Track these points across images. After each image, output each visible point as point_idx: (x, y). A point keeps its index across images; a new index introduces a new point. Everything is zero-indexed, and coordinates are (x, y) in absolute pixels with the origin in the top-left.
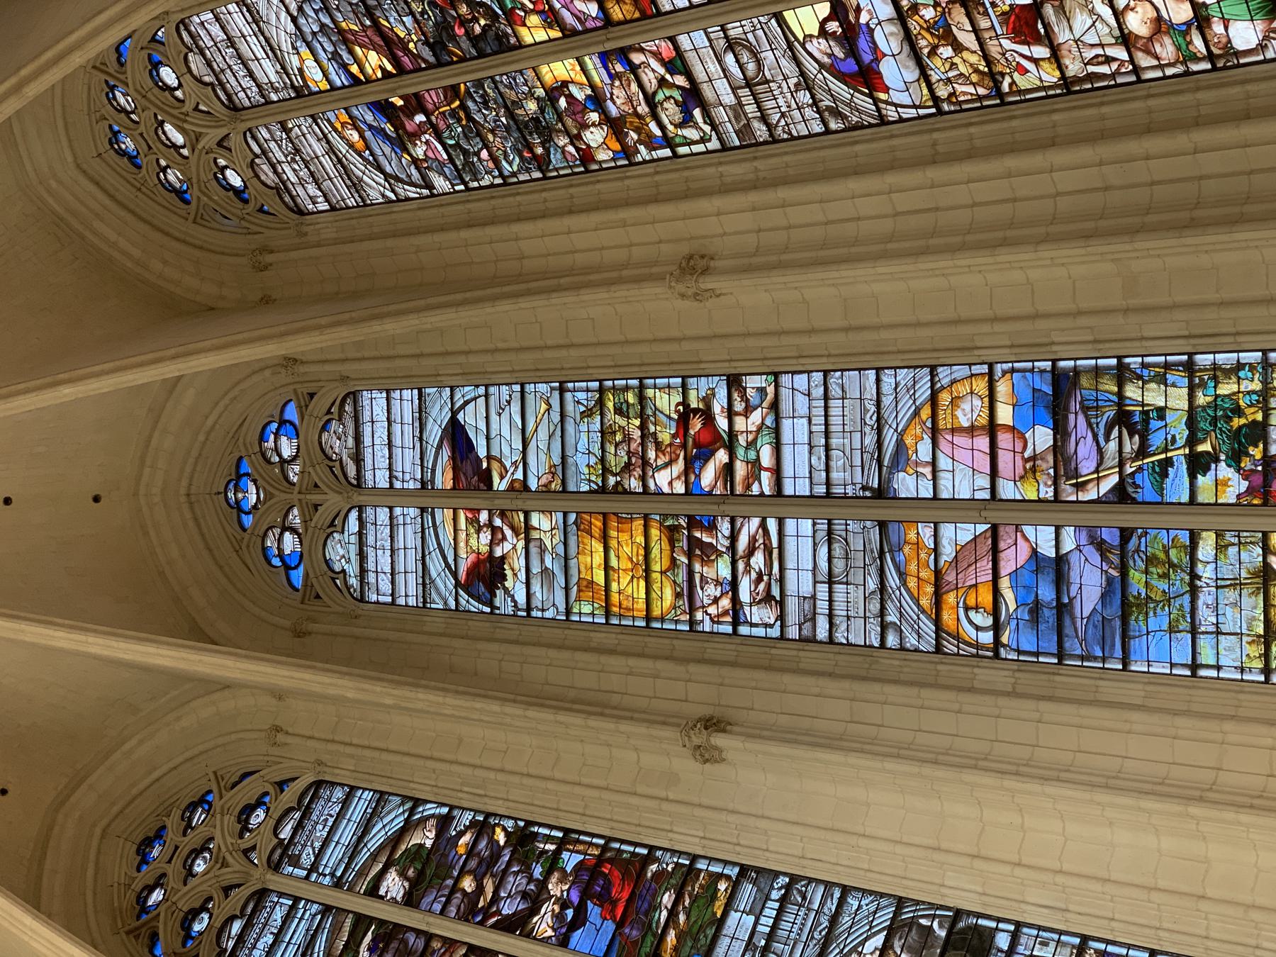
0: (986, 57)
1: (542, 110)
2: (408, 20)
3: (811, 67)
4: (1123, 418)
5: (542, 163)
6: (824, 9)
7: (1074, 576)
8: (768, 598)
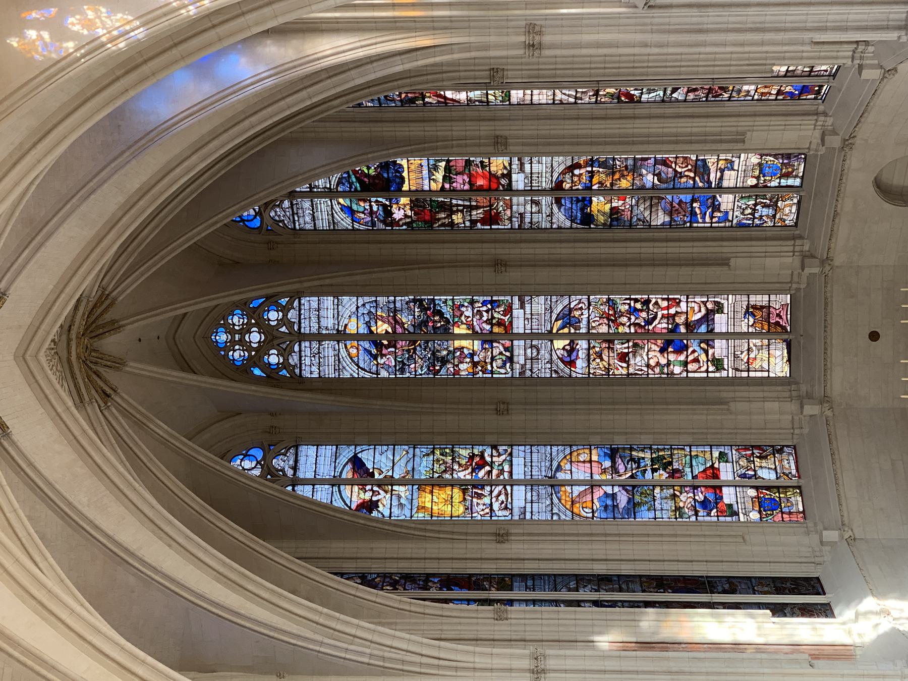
0: (609, 365)
1: (448, 354)
2: (411, 317)
3: (555, 357)
4: (632, 459)
5: (437, 372)
6: (568, 342)
7: (618, 498)
8: (506, 508)
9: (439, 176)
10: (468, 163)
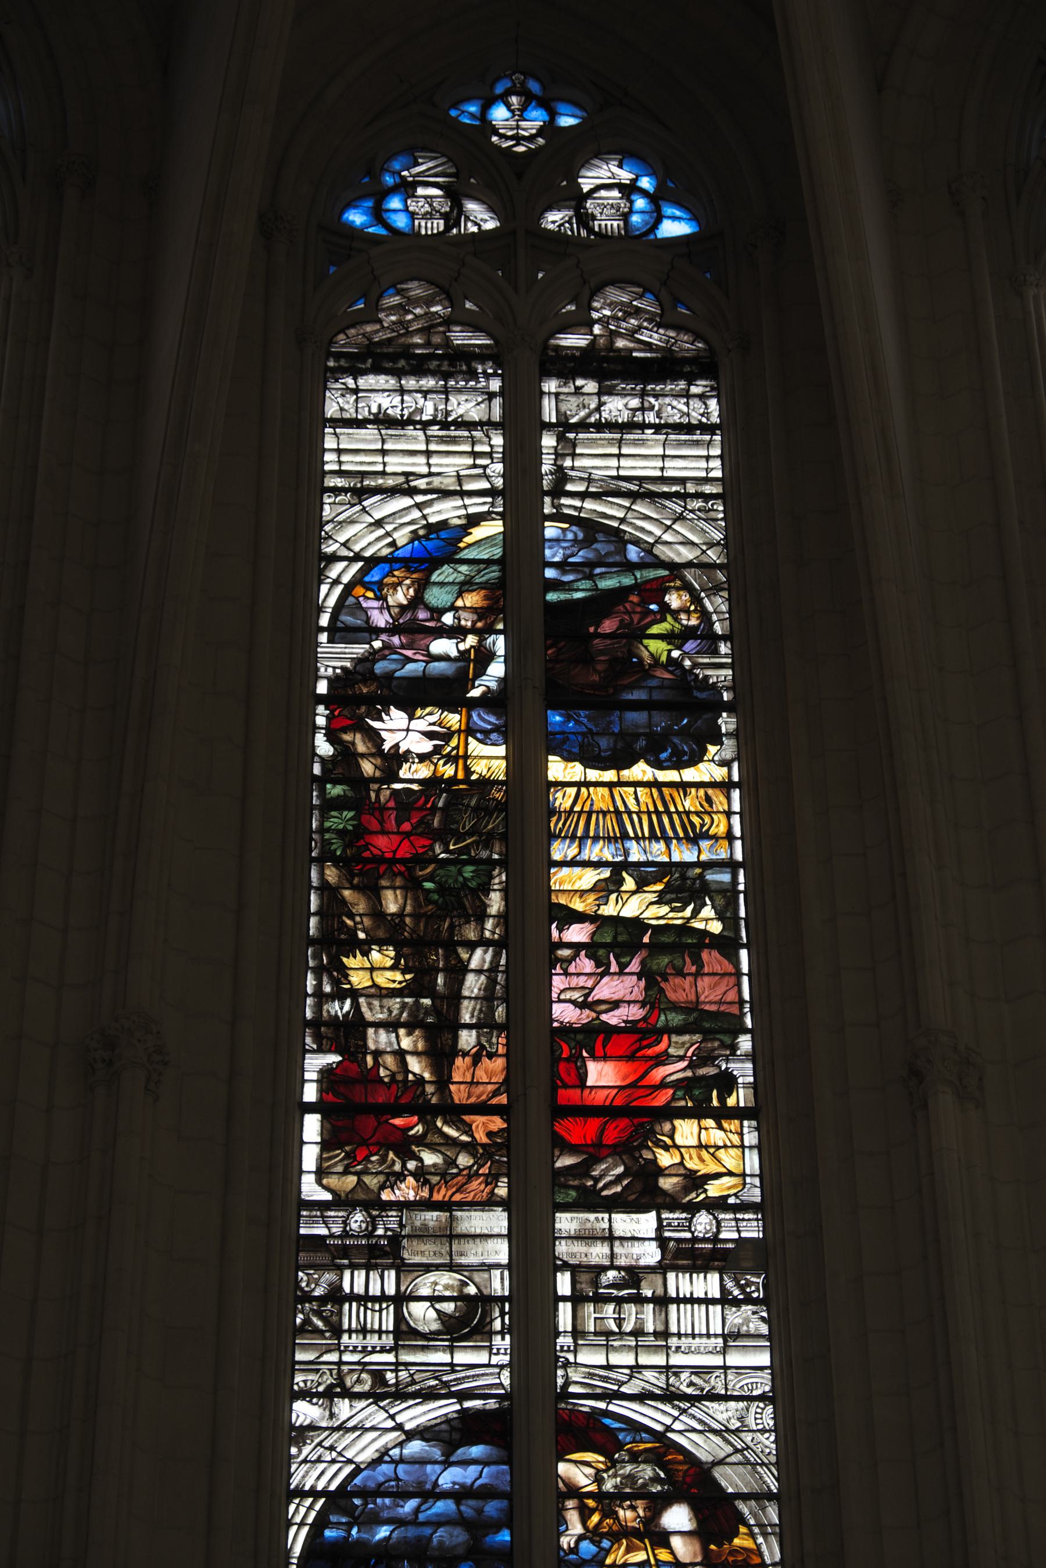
9: (634, 905)
10: (716, 1027)
